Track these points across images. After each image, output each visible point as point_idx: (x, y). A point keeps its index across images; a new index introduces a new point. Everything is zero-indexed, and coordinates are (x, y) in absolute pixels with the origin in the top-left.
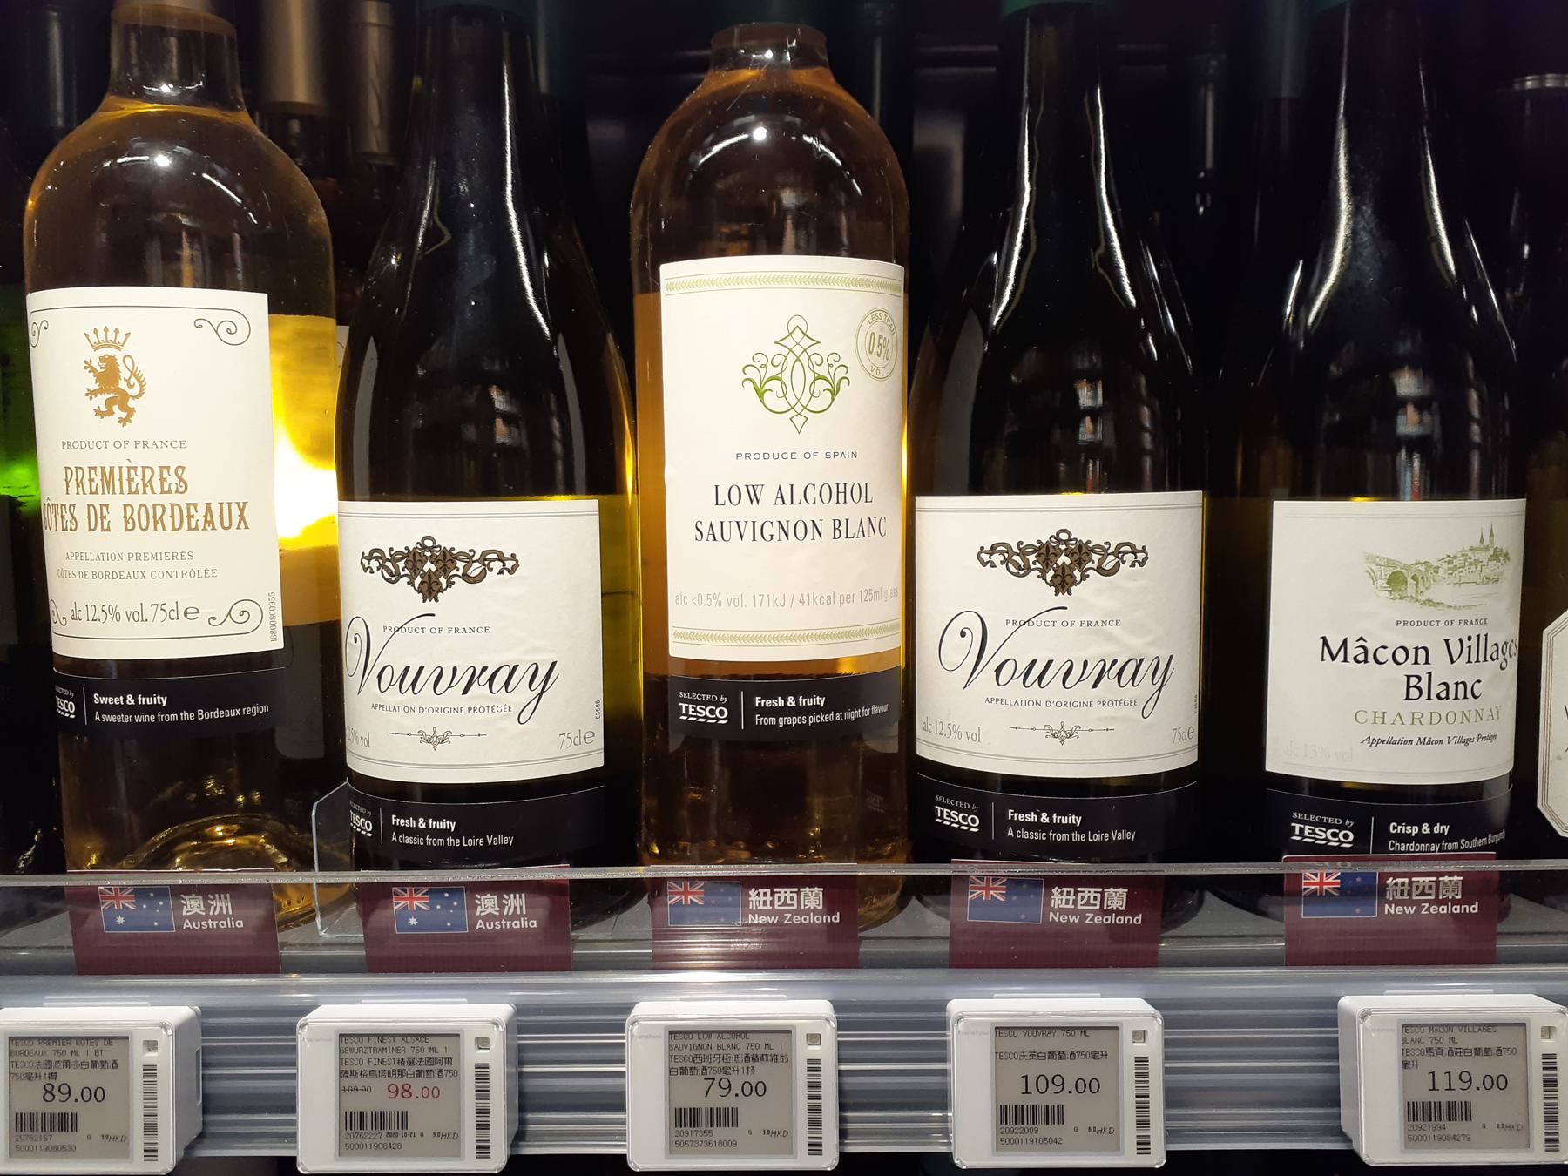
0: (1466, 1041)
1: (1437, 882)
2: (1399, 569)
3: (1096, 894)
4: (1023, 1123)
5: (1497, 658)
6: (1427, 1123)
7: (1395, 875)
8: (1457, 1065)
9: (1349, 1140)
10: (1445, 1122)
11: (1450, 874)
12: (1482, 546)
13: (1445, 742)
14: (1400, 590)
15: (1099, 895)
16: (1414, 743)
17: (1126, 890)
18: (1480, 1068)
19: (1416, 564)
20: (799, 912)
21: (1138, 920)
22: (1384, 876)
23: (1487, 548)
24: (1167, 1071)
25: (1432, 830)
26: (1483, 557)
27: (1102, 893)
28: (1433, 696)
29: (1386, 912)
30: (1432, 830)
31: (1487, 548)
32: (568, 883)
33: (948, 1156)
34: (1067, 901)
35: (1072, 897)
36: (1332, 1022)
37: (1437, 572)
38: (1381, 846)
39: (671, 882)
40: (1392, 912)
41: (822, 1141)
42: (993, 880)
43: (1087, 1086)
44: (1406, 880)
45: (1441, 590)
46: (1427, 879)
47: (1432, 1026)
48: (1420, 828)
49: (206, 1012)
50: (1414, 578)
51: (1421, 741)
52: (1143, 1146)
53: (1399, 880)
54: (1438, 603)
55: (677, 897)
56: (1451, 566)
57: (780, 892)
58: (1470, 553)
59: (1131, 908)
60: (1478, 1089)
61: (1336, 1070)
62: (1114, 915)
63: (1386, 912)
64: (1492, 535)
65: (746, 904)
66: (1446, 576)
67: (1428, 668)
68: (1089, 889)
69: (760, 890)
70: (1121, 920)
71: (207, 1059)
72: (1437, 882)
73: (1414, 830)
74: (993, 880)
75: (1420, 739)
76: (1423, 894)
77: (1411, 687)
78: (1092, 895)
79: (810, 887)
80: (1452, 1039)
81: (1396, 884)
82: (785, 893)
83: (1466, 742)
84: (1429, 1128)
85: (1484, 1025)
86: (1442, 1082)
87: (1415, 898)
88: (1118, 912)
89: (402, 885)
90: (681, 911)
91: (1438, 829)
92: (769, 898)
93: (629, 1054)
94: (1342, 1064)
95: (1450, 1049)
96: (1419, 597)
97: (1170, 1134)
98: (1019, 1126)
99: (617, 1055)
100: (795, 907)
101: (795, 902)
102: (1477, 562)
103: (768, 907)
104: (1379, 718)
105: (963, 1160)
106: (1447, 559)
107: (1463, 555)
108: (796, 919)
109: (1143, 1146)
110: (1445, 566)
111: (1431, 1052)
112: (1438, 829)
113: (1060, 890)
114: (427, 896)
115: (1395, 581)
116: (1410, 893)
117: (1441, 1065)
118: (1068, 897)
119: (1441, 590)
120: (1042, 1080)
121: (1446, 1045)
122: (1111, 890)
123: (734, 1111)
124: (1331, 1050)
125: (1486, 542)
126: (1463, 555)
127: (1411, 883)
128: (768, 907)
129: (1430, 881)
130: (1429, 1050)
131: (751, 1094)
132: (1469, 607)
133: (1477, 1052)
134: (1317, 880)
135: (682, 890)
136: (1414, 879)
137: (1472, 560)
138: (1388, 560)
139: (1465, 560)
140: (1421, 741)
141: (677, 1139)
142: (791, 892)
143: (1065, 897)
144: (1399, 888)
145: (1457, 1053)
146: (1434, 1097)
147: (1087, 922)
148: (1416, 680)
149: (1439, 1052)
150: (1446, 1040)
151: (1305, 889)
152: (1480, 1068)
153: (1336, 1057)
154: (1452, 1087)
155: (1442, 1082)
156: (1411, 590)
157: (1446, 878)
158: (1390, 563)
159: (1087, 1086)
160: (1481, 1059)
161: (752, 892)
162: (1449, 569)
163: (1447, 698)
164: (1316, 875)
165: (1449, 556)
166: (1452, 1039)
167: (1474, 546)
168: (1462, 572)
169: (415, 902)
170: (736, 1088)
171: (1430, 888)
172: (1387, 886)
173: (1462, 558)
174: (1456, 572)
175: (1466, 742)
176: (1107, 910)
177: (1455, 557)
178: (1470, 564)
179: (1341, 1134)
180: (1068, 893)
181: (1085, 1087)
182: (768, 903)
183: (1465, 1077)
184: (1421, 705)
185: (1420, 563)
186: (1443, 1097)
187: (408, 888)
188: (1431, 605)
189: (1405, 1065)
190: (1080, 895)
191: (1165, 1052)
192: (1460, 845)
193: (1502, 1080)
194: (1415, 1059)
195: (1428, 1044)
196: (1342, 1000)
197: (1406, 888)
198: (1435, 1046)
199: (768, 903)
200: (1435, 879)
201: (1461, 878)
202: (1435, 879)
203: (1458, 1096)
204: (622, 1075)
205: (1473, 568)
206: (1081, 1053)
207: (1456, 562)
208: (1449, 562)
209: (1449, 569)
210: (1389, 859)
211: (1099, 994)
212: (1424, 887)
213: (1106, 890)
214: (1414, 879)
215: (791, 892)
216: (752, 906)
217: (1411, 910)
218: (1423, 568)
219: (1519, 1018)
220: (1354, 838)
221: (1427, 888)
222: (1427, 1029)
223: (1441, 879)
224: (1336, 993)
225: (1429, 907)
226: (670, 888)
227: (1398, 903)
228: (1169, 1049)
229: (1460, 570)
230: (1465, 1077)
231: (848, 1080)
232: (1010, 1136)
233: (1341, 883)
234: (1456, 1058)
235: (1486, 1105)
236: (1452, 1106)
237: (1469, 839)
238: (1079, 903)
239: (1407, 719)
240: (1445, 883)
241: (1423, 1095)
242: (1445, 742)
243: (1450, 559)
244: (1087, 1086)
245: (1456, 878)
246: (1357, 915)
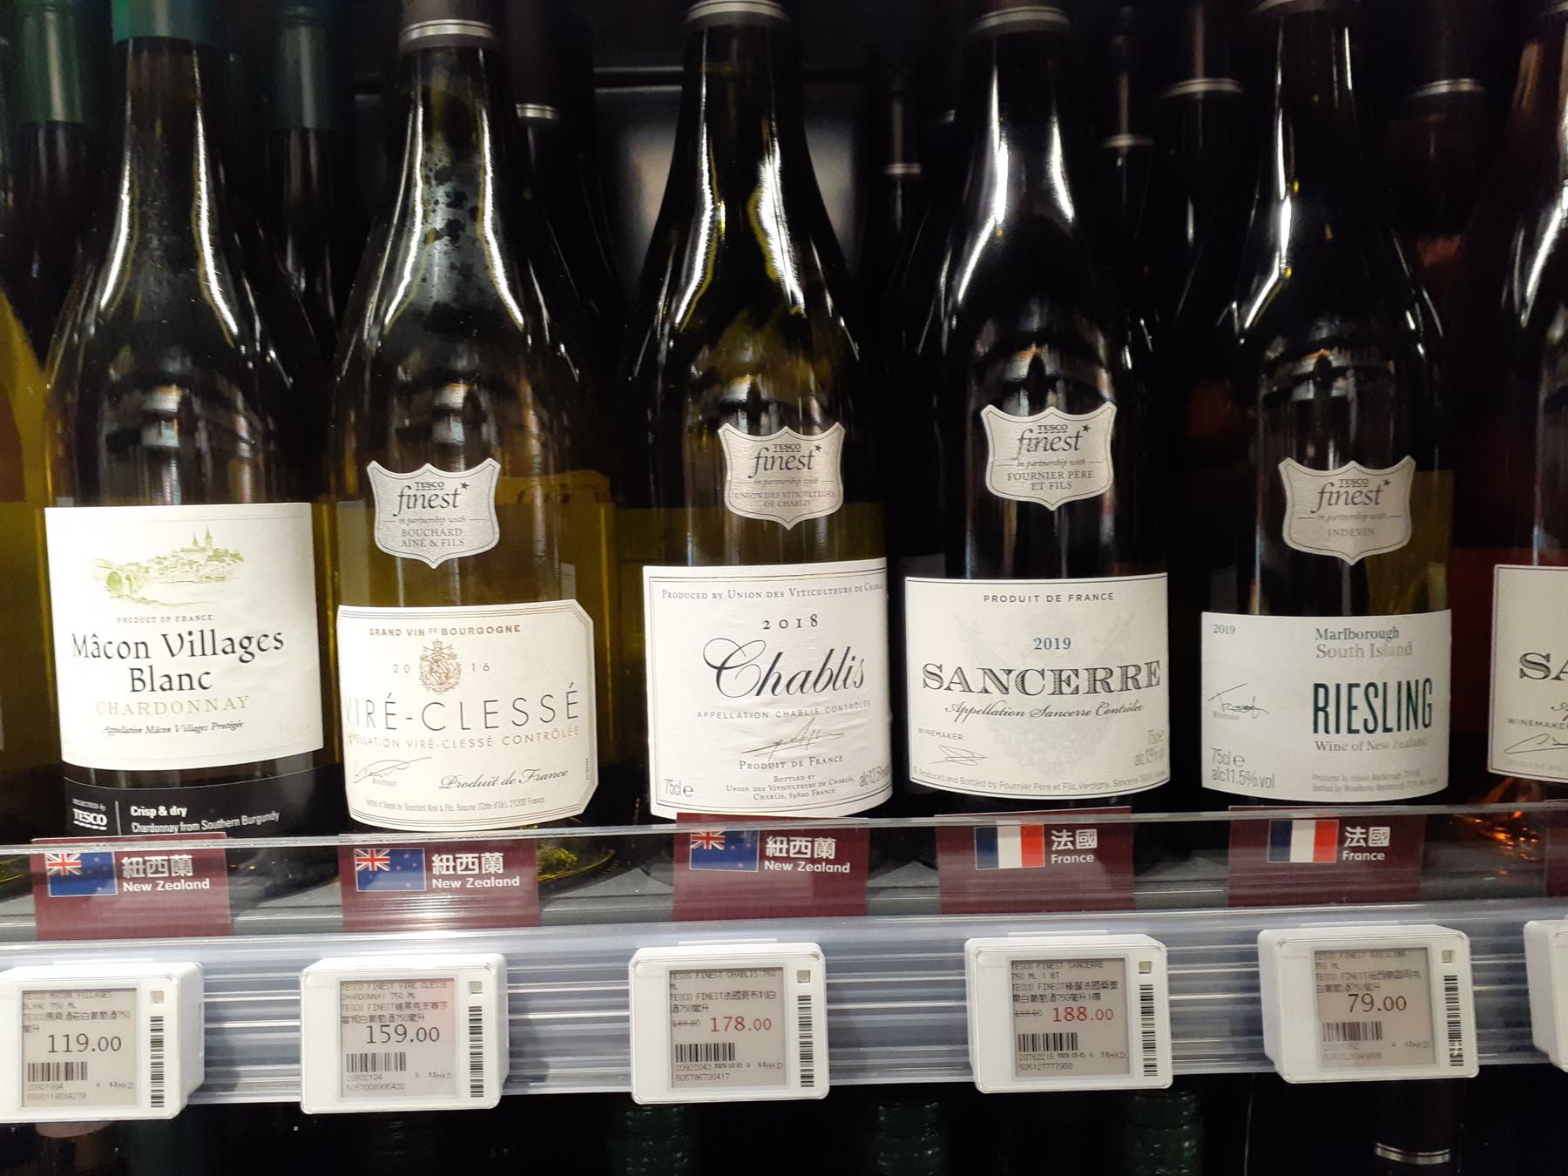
0: (84, 1005)
1: (169, 861)
2: (114, 570)
3: (474, 860)
4: (697, 1061)
5: (233, 652)
6: (46, 1083)
7: (130, 855)
8: (74, 1028)
9: (1272, 1063)
10: (62, 1081)
11: (180, 852)
12: (196, 548)
13: (173, 729)
14: (117, 589)
15: (476, 861)
16: (143, 731)
17: (502, 854)
18: (96, 1030)
19: (131, 564)
20: (480, 876)
21: (846, 868)
22: (120, 855)
23: (204, 550)
24: (830, 1013)
25: (168, 813)
26: (200, 558)
27: (479, 858)
28: (157, 687)
29: (766, 868)
30: (168, 813)
31: (204, 550)
32: (224, 855)
33: (628, 1095)
34: (448, 867)
35: (451, 864)
36: (1252, 957)
37: (147, 572)
38: (127, 830)
39: (358, 850)
40: (772, 868)
41: (484, 1083)
42: (378, 851)
43: (428, 1034)
44: (140, 860)
45: (154, 588)
46: (159, 858)
47: (53, 993)
48: (158, 810)
49: (207, 970)
50: (128, 578)
51: (150, 730)
52: (807, 1079)
53: (134, 860)
54: (152, 601)
55: (365, 863)
56: (161, 566)
57: (461, 858)
58: (181, 554)
59: (839, 860)
60: (93, 1050)
61: (1257, 1001)
62: (493, 878)
63: (766, 868)
64: (208, 536)
65: (430, 868)
66: (158, 576)
67: (147, 663)
68: (801, 838)
69: (443, 856)
70: (831, 869)
71: (213, 1014)
72: (169, 861)
73: (152, 813)
74: (378, 851)
75: (148, 727)
76: (156, 872)
77: (137, 679)
78: (470, 860)
79: (491, 853)
80: (71, 1004)
81: (131, 863)
82: (467, 858)
83: (198, 730)
84: (48, 1088)
85: (100, 990)
86: (60, 1044)
87: (150, 876)
88: (828, 861)
89: (364, 847)
90: (368, 877)
91: (175, 811)
92: (785, 846)
93: (305, 1009)
94: (1264, 995)
95: (69, 1014)
96: (134, 596)
97: (833, 1071)
98: (694, 1063)
99: (292, 1009)
100: (477, 872)
101: (476, 867)
102: (191, 563)
103: (451, 872)
104: (113, 708)
105: (640, 1098)
106: (157, 560)
107: (174, 556)
108: (478, 883)
109: (807, 1079)
110: (156, 566)
111: (51, 1017)
112: (175, 811)
113: (439, 858)
114: (388, 857)
115: (113, 580)
116: (145, 871)
117: (60, 1028)
118: (448, 864)
119: (154, 588)
120: (421, 1032)
121: (65, 1011)
122: (488, 855)
123: (731, 1047)
124: (1251, 983)
125: (202, 543)
126: (174, 556)
127: (145, 862)
128: (451, 872)
129: (162, 860)
130: (50, 1015)
131: (425, 1039)
132: (187, 604)
133: (94, 1015)
134: (59, 861)
135: (368, 857)
136: (147, 858)
137: (185, 561)
138: (107, 562)
139: (177, 561)
140: (150, 730)
141: (348, 1083)
142: (473, 858)
143: (445, 864)
144: (135, 867)
145: (75, 1017)
146: (53, 1059)
147: (799, 869)
148: (139, 672)
149: (59, 1016)
150: (66, 1005)
151: (50, 869)
152: (96, 1030)
153: (1257, 989)
154: (55, 1050)
155: (60, 1044)
156: (125, 589)
157: (176, 857)
158: (107, 565)
159: (1395, 1004)
160: (99, 1022)
161: (436, 858)
162: (159, 570)
163: (171, 689)
164: (57, 855)
165: (158, 558)
166: (71, 1004)
167: (186, 547)
168: (174, 572)
169: (377, 864)
170: (1378, 1003)
171: (163, 866)
172: (123, 865)
173: (174, 559)
174: (168, 572)
175: (198, 730)
176: (818, 859)
177: (165, 558)
178: (184, 564)
179: (1532, 1049)
180: (448, 860)
181: (112, 1043)
182: (141, 871)
183: (82, 1039)
184: (145, 695)
185: (131, 564)
186: (61, 1058)
187: (369, 850)
188: (147, 604)
189: (26, 1029)
190: (458, 861)
191: (827, 995)
192: (201, 826)
193: (116, 1042)
194: (35, 1022)
195: (48, 1009)
196: (1262, 933)
197: (141, 867)
198: (55, 1011)
199: (141, 871)
200: (166, 858)
201: (191, 857)
202: (166, 858)
203: (75, 1058)
204: (297, 1029)
205: (187, 568)
206: (122, 1013)
207: (166, 563)
208: (159, 563)
209: (159, 570)
210: (130, 840)
211: (775, 940)
212: (157, 865)
213: (482, 855)
214: (147, 858)
215: (473, 858)
216: (769, 853)
217: (147, 887)
218: (134, 568)
219: (1421, 943)
220: (107, 818)
221: (160, 866)
222: (1338, 955)
223: (171, 857)
224: (1257, 926)
225: (805, 866)
226: (49, 860)
227: (134, 880)
228: (831, 993)
229: (172, 570)
230: (82, 1039)
231: (518, 1029)
232: (685, 1073)
233: (82, 863)
234: (73, 1022)
235: (99, 1064)
236: (69, 1067)
237: (213, 819)
238: (459, 868)
239: (135, 709)
240: (176, 862)
241: (41, 1056)
242: (173, 729)
243: (160, 560)
244: (428, 1034)
245: (185, 857)
246: (738, 872)
